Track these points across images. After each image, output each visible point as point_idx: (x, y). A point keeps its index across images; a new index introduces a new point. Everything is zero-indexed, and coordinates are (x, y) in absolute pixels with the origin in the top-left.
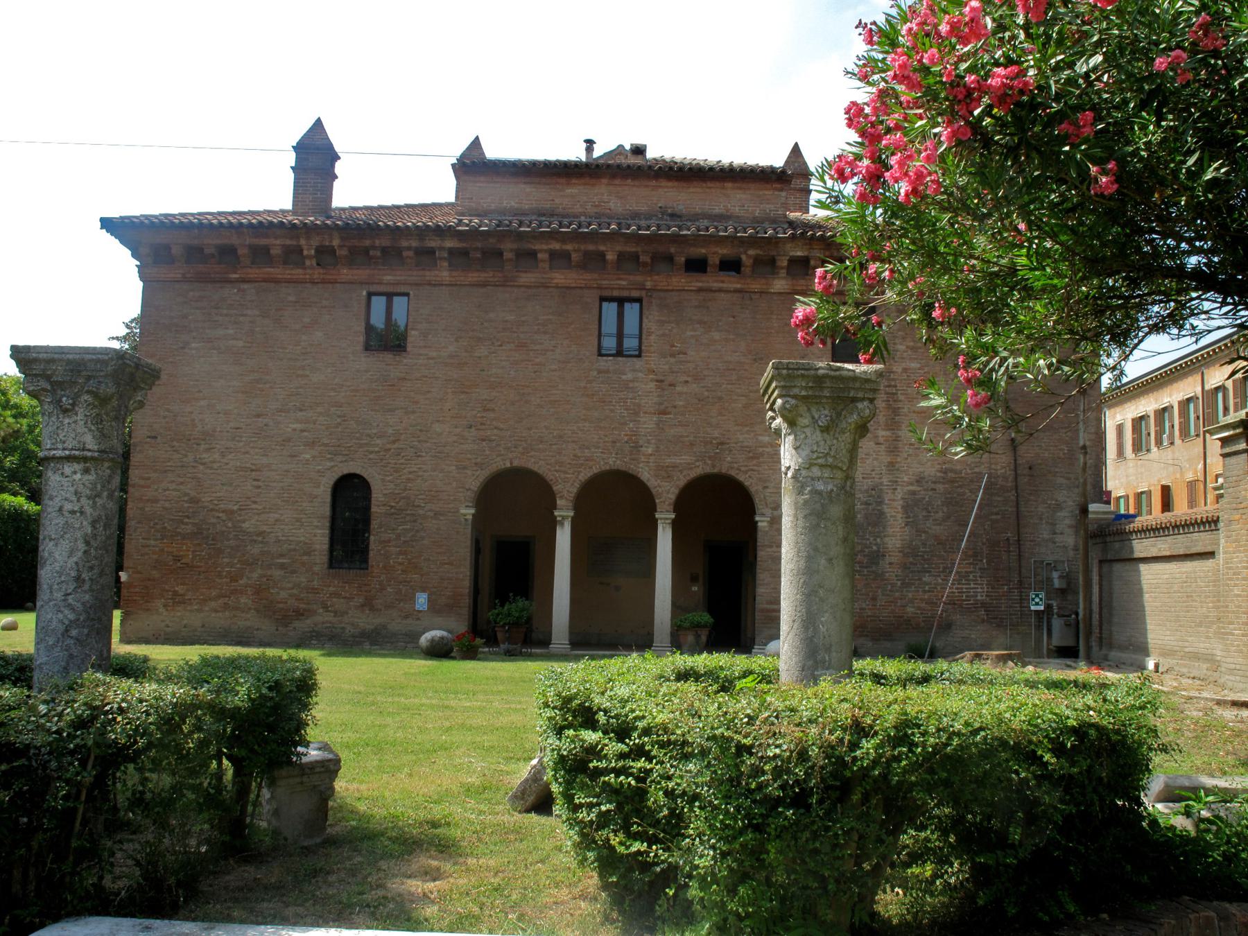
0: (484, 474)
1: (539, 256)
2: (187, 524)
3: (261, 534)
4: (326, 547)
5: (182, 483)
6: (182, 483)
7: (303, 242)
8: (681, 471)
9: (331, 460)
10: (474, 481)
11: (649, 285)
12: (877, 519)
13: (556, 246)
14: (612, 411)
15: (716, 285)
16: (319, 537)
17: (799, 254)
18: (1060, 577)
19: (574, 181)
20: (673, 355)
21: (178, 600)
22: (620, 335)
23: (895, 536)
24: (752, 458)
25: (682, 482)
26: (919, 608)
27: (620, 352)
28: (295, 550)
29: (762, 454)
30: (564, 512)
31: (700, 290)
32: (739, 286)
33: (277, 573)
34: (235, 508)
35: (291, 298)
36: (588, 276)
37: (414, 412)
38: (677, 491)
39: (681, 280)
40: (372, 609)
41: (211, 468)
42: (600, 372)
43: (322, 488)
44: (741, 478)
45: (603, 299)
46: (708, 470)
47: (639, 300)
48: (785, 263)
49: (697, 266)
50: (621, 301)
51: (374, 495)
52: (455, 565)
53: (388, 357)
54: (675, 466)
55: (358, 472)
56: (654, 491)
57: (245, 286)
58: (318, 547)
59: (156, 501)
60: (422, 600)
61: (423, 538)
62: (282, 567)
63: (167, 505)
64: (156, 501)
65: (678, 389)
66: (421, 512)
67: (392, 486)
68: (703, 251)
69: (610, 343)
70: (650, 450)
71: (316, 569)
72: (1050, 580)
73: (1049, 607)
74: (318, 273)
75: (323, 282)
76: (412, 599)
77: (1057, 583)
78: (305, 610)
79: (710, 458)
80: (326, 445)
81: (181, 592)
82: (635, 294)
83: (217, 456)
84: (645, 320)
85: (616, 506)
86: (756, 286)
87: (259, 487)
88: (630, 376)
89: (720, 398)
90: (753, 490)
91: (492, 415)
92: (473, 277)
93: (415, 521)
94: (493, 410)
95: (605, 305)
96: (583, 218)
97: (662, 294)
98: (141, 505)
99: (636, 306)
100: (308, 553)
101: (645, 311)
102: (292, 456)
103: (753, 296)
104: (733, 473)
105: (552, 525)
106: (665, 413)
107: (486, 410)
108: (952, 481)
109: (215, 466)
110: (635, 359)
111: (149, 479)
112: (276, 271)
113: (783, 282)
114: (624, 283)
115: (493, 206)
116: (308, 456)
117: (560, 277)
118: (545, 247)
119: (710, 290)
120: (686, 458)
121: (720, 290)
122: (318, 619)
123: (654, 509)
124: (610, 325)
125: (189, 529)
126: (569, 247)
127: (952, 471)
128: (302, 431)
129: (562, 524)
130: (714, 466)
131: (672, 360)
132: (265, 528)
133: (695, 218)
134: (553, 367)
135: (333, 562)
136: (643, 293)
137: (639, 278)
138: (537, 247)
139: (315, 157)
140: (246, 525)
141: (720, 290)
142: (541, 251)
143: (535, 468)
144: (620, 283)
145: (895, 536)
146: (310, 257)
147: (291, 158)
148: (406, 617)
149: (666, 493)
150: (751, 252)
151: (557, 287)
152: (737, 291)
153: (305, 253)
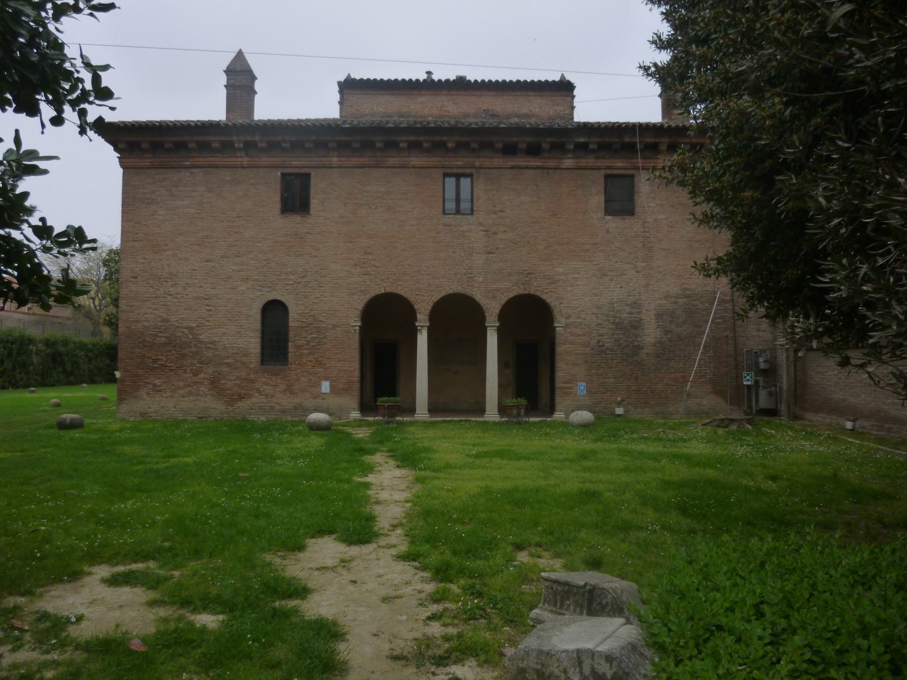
0: (367, 298)
1: (402, 145)
2: (161, 337)
3: (213, 342)
4: (259, 351)
5: (156, 309)
6: (156, 309)
7: (235, 138)
8: (503, 293)
9: (260, 290)
10: (360, 302)
11: (477, 164)
12: (637, 325)
13: (412, 138)
14: (454, 252)
15: (524, 164)
16: (252, 343)
17: (582, 140)
18: (765, 361)
19: (423, 92)
20: (495, 213)
21: (157, 390)
22: (458, 200)
23: (651, 335)
24: (552, 283)
25: (504, 301)
26: (667, 384)
27: (458, 211)
28: (237, 353)
29: (558, 281)
30: (422, 321)
31: (513, 168)
32: (540, 164)
33: (225, 369)
34: (194, 325)
35: (228, 178)
36: (435, 159)
37: (316, 256)
39: (499, 161)
40: (292, 393)
41: (176, 298)
42: (445, 225)
43: (254, 311)
44: (544, 297)
45: (446, 175)
46: (521, 292)
47: (470, 175)
48: (572, 147)
49: (510, 150)
50: (458, 176)
51: (290, 314)
52: (349, 362)
53: (297, 218)
55: (279, 298)
56: (484, 308)
57: (196, 170)
58: (253, 351)
59: (138, 322)
60: (325, 387)
61: (325, 343)
62: (229, 365)
63: (146, 324)
64: (138, 322)
65: (500, 236)
66: (324, 325)
67: (303, 307)
68: (515, 139)
69: (451, 206)
70: (481, 280)
71: (252, 366)
72: (757, 363)
73: (757, 382)
74: (246, 161)
75: (250, 167)
76: (319, 385)
77: (762, 366)
78: (245, 395)
79: (522, 284)
80: (256, 280)
81: (158, 384)
82: (467, 171)
83: (180, 290)
84: (475, 189)
85: (457, 318)
86: (552, 163)
87: (210, 310)
88: (466, 228)
89: (528, 242)
91: (370, 257)
92: (355, 161)
93: (319, 332)
94: (371, 254)
95: (447, 179)
96: (430, 119)
97: (487, 171)
98: (128, 325)
99: (469, 180)
100: (246, 355)
101: (475, 181)
102: (232, 289)
103: (550, 171)
104: (538, 294)
105: (413, 333)
106: (490, 253)
107: (366, 253)
108: (688, 297)
109: (179, 296)
110: (469, 217)
111: (132, 306)
112: (217, 160)
113: (570, 161)
114: (460, 163)
115: (367, 111)
116: (244, 288)
117: (415, 160)
118: (404, 138)
119: (520, 168)
121: (527, 167)
122: (254, 400)
123: (483, 318)
124: (450, 193)
125: (163, 340)
126: (421, 139)
127: (688, 289)
128: (239, 271)
129: (421, 330)
130: (525, 289)
131: (495, 216)
132: (216, 339)
133: (508, 116)
134: (413, 223)
135: (263, 361)
136: (474, 171)
137: (471, 160)
138: (399, 138)
139: (240, 80)
140: (202, 337)
141: (527, 167)
142: (403, 141)
143: (402, 293)
144: (458, 162)
145: (651, 335)
146: (240, 149)
147: (224, 79)
148: (315, 398)
149: (492, 309)
150: (548, 140)
151: (414, 167)
152: (538, 168)
153: (236, 145)
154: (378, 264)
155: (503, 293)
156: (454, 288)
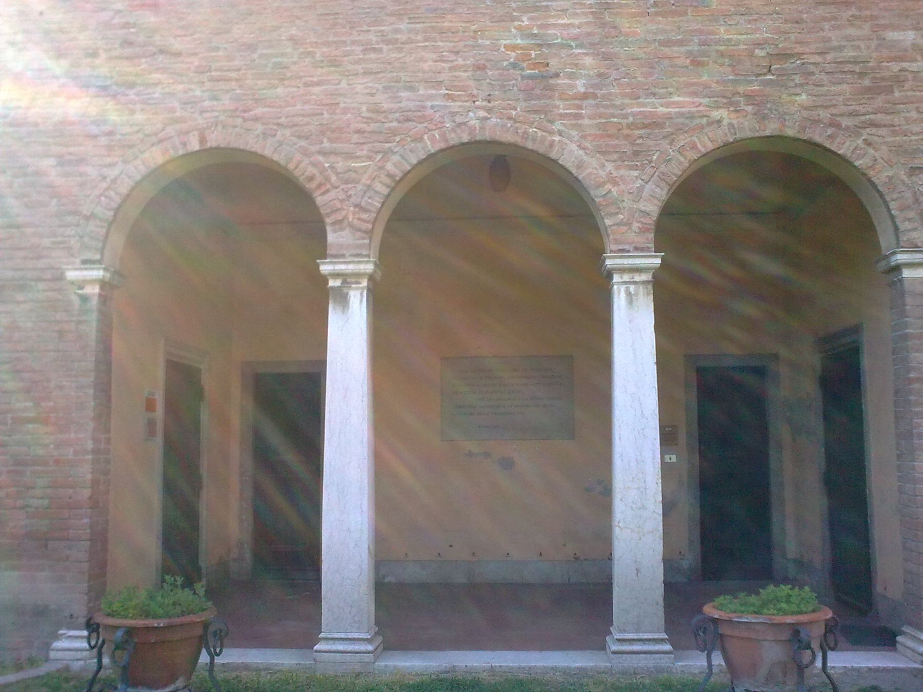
8: (671, 138)
29: (898, 80)
30: (350, 261)
38: (663, 193)
44: (844, 147)
54: (653, 124)
56: (597, 194)
70: (580, 86)
90: (880, 177)
120: (680, 103)
129: (343, 300)
143: (267, 150)
149: (629, 200)
154: (177, 45)
155: (671, 138)
156: (473, 119)
